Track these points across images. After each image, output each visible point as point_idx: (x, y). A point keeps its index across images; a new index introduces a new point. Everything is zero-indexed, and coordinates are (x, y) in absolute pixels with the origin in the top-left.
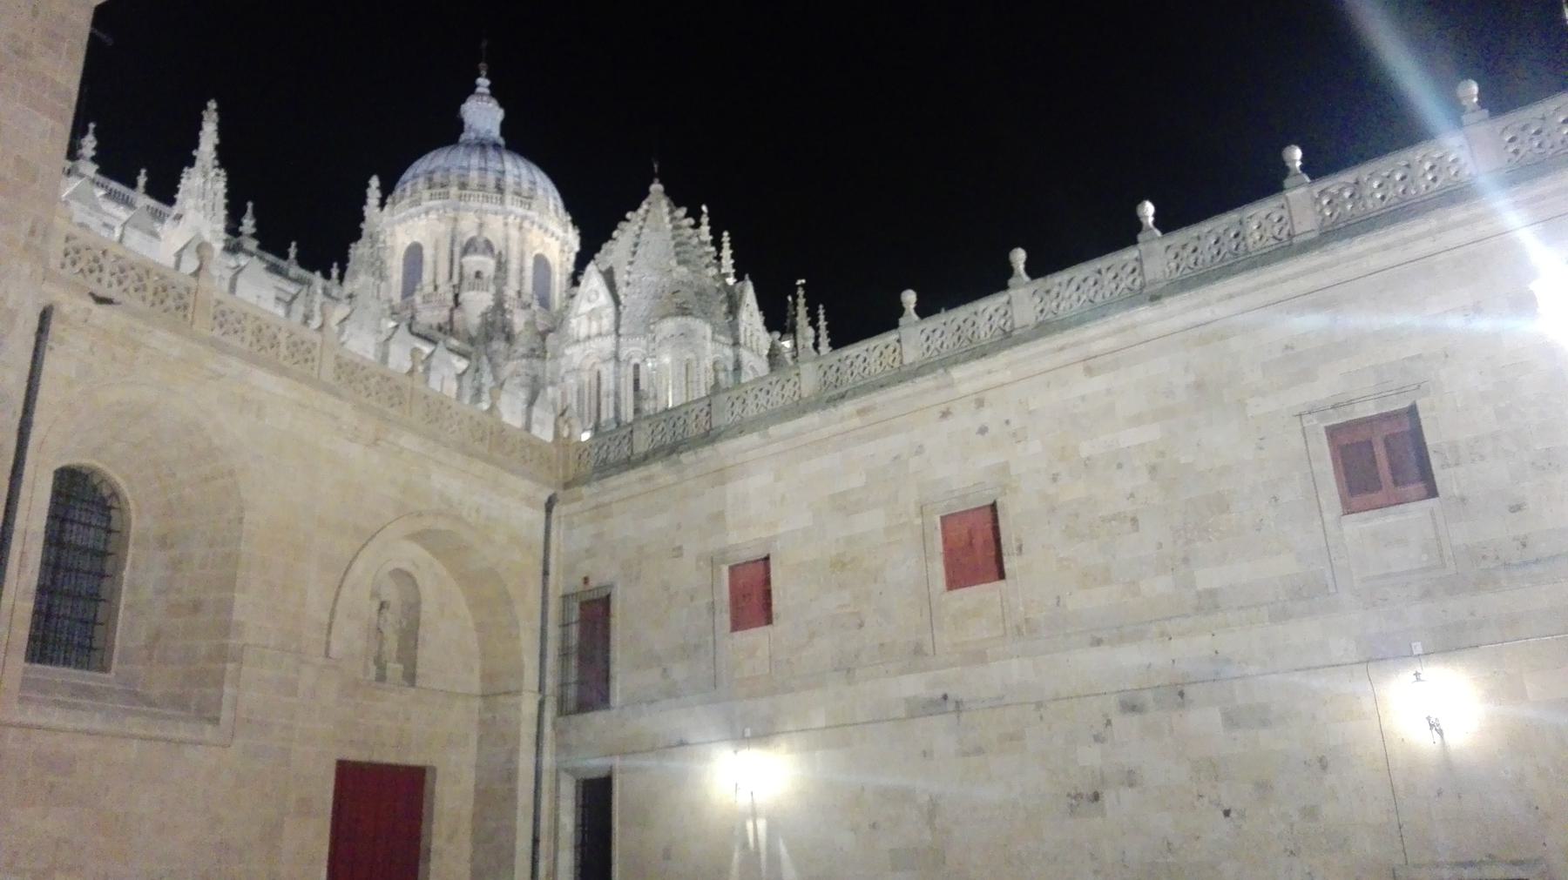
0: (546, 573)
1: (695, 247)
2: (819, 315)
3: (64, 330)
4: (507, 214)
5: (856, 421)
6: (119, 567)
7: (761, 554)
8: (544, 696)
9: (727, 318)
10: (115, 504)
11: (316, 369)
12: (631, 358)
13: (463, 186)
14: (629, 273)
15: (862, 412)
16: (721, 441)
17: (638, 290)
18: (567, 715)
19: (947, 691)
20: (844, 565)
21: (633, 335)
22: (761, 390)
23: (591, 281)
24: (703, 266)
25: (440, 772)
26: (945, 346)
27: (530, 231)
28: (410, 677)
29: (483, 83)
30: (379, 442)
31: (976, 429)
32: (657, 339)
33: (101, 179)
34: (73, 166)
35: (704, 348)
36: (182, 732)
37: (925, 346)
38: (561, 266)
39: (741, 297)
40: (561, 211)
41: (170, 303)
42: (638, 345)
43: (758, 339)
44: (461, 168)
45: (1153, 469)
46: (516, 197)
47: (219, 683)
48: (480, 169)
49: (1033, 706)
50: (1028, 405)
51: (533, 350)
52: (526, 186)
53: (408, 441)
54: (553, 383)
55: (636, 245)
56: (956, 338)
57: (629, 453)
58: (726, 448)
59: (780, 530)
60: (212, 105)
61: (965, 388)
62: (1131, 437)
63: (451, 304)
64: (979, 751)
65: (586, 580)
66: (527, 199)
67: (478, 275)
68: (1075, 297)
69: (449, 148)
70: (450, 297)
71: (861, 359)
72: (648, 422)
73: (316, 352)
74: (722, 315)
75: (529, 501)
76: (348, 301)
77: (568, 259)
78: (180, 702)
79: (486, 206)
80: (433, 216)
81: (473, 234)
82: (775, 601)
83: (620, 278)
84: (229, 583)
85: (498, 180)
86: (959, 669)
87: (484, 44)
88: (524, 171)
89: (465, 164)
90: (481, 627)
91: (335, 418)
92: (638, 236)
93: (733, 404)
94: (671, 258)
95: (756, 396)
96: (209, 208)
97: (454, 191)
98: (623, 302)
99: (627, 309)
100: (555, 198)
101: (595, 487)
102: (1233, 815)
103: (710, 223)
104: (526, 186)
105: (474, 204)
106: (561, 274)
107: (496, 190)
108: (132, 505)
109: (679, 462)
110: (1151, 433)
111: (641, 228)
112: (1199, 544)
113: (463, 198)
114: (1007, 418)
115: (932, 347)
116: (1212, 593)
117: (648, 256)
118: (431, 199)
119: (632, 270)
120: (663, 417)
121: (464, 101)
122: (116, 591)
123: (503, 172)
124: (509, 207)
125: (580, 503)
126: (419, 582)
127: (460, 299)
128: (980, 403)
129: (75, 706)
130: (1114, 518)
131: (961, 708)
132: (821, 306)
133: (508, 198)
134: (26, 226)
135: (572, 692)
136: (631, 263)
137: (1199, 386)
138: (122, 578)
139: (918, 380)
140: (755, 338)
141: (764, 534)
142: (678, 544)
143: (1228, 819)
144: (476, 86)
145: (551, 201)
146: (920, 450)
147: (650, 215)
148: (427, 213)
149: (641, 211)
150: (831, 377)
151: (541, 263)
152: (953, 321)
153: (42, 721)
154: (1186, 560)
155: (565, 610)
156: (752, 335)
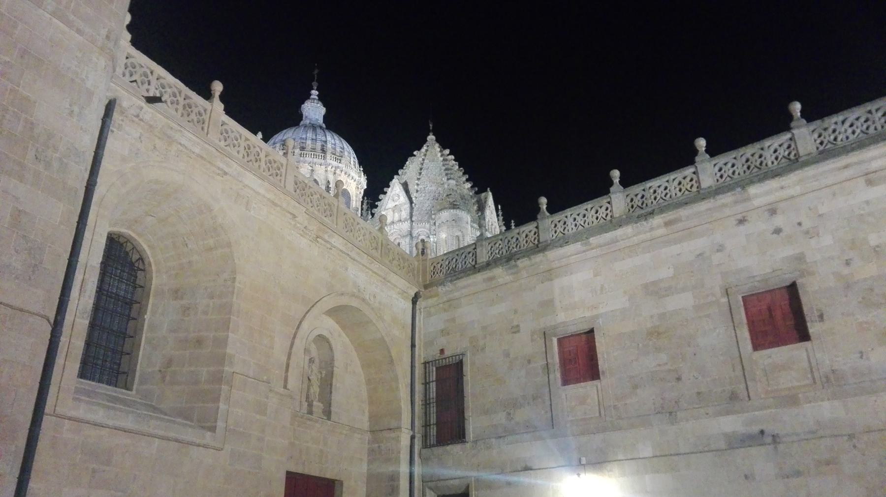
0: (413, 346)
1: (456, 171)
2: (511, 226)
4: (327, 165)
5: (662, 231)
6: (142, 311)
7: (586, 327)
8: (414, 432)
9: (477, 214)
10: (141, 267)
11: (283, 182)
12: (419, 235)
13: (303, 149)
14: (418, 185)
15: (667, 224)
16: (552, 249)
17: (423, 195)
18: (430, 447)
20: (659, 334)
21: (421, 221)
22: (578, 215)
23: (395, 189)
24: (462, 182)
25: (345, 484)
26: (737, 173)
27: (340, 175)
28: (328, 413)
29: (315, 93)
30: (318, 239)
32: (437, 224)
35: (467, 229)
36: (189, 434)
37: (719, 174)
38: (356, 197)
39: (485, 202)
40: (357, 165)
41: (193, 116)
42: (424, 228)
43: (495, 228)
44: (301, 138)
47: (217, 400)
48: (312, 139)
49: (846, 438)
52: (338, 150)
53: (337, 241)
55: (421, 169)
56: (745, 167)
57: (473, 263)
58: (552, 254)
59: (602, 310)
61: (756, 202)
64: (798, 474)
65: (442, 351)
66: (339, 159)
68: (850, 130)
69: (294, 129)
71: (662, 188)
72: (488, 241)
73: (283, 170)
74: (474, 211)
75: (403, 293)
77: (360, 193)
78: (185, 414)
79: (315, 160)
82: (600, 362)
83: (412, 188)
84: (225, 325)
85: (323, 146)
86: (773, 411)
87: (316, 72)
88: (337, 142)
89: (304, 136)
90: (369, 382)
91: (294, 216)
92: (422, 164)
93: (556, 226)
94: (443, 177)
95: (575, 219)
98: (414, 202)
99: (417, 206)
100: (354, 158)
101: (449, 287)
104: (338, 150)
105: (308, 159)
106: (356, 202)
107: (321, 151)
108: (153, 268)
109: (516, 266)
111: (423, 160)
113: (302, 155)
114: (799, 221)
115: (725, 176)
117: (429, 175)
119: (419, 183)
120: (500, 237)
121: (303, 103)
122: (138, 330)
123: (326, 142)
124: (329, 161)
125: (435, 299)
126: (334, 346)
128: (773, 212)
129: (113, 408)
131: (778, 440)
132: (513, 221)
133: (328, 156)
134: (104, 32)
135: (433, 431)
136: (418, 179)
138: (144, 320)
139: (718, 197)
140: (493, 227)
141: (588, 314)
142: (515, 323)
144: (311, 95)
145: (352, 159)
147: (428, 153)
149: (423, 150)
150: (637, 201)
152: (742, 156)
153: (90, 417)
155: (426, 374)
156: (492, 225)
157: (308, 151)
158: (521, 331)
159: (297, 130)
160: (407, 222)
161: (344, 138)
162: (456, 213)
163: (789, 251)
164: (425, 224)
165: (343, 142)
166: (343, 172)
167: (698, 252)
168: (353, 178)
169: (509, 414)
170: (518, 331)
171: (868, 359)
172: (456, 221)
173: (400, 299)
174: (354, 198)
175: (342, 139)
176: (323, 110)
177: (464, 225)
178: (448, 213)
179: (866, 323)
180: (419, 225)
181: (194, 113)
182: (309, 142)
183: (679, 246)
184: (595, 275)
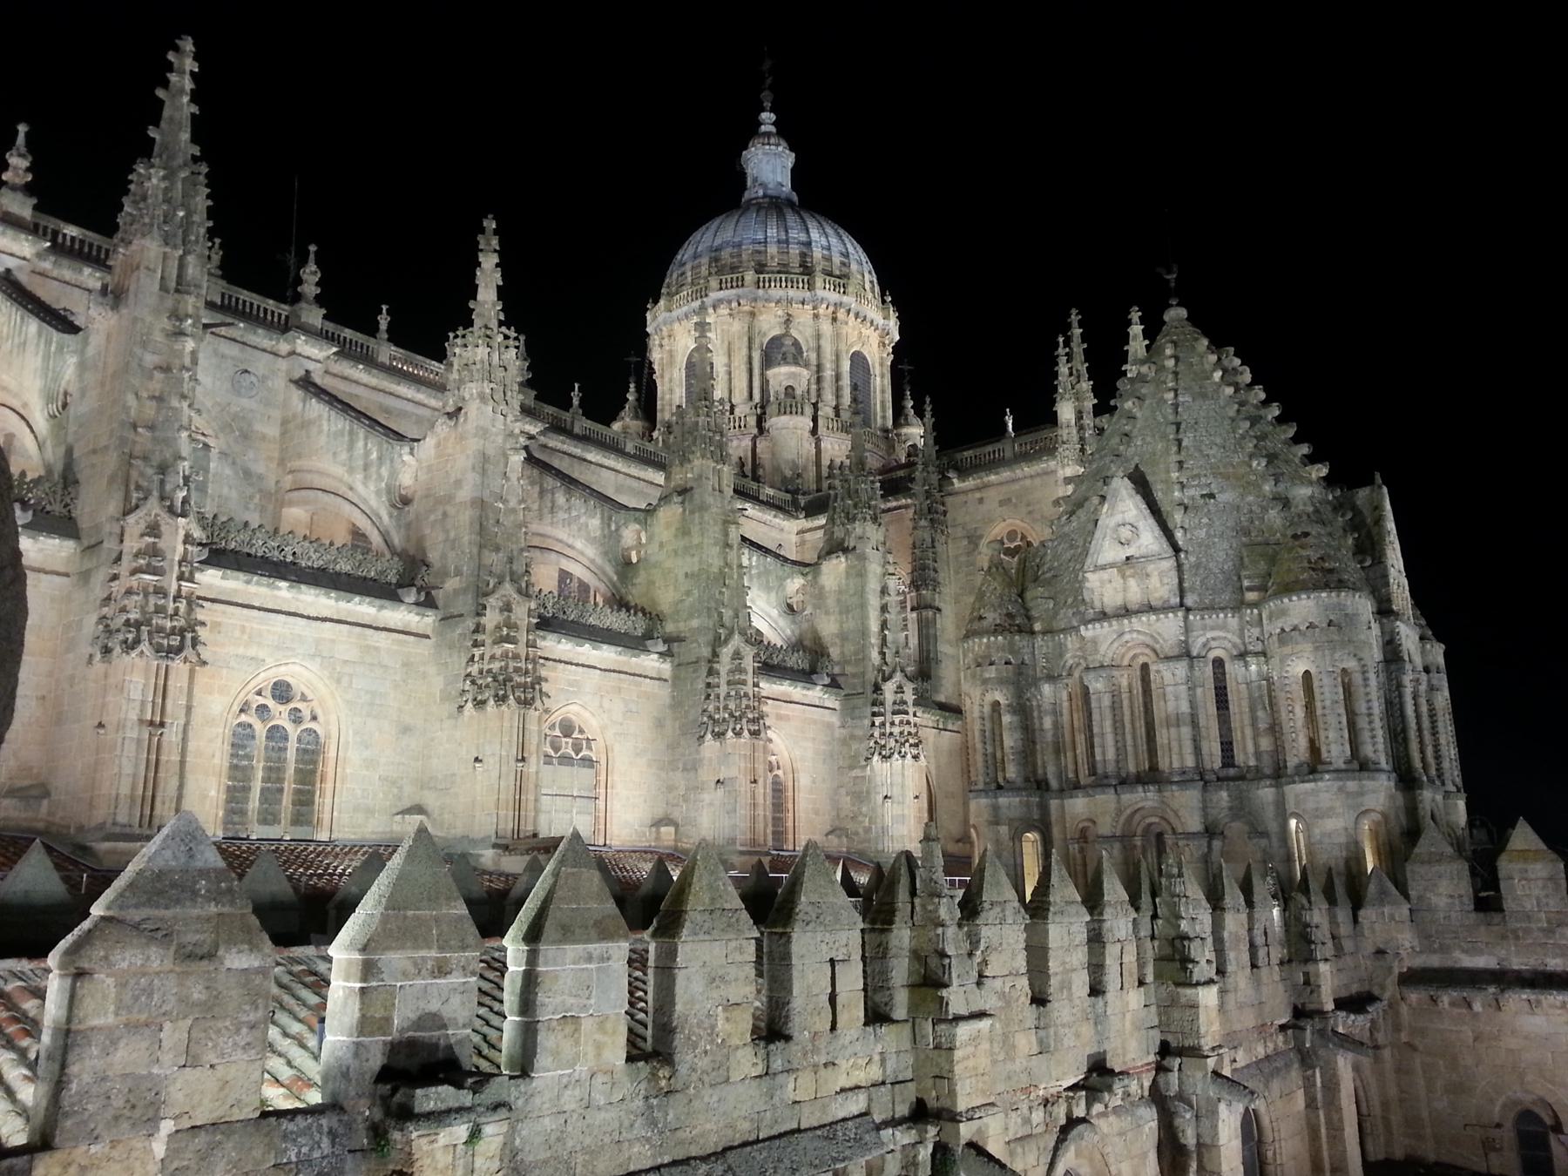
13: (760, 268)
21: (1212, 608)
23: (1121, 506)
27: (847, 323)
29: (767, 117)
33: (330, 327)
34: (291, 312)
42: (1224, 627)
44: (755, 242)
46: (828, 278)
48: (779, 242)
51: (1010, 615)
52: (837, 259)
54: (1051, 678)
60: (490, 224)
63: (755, 431)
66: (840, 279)
67: (790, 390)
70: (752, 421)
76: (680, 499)
79: (792, 293)
80: (723, 310)
81: (777, 332)
85: (803, 255)
87: (767, 65)
88: (834, 240)
89: (760, 236)
96: (499, 396)
97: (750, 276)
103: (1142, 320)
104: (837, 259)
105: (776, 292)
106: (882, 376)
118: (721, 289)
121: (746, 148)
123: (809, 244)
124: (820, 293)
127: (767, 425)
133: (819, 282)
145: (867, 276)
148: (715, 308)
151: (858, 360)
157: (773, 272)
159: (742, 220)
160: (1176, 616)
161: (846, 229)
162: (1335, 600)
164: (1226, 616)
165: (844, 238)
166: (852, 315)
168: (872, 323)
172: (1340, 628)
174: (878, 371)
175: (841, 231)
176: (789, 159)
177: (1362, 637)
178: (1311, 603)
180: (1208, 621)
182: (772, 249)
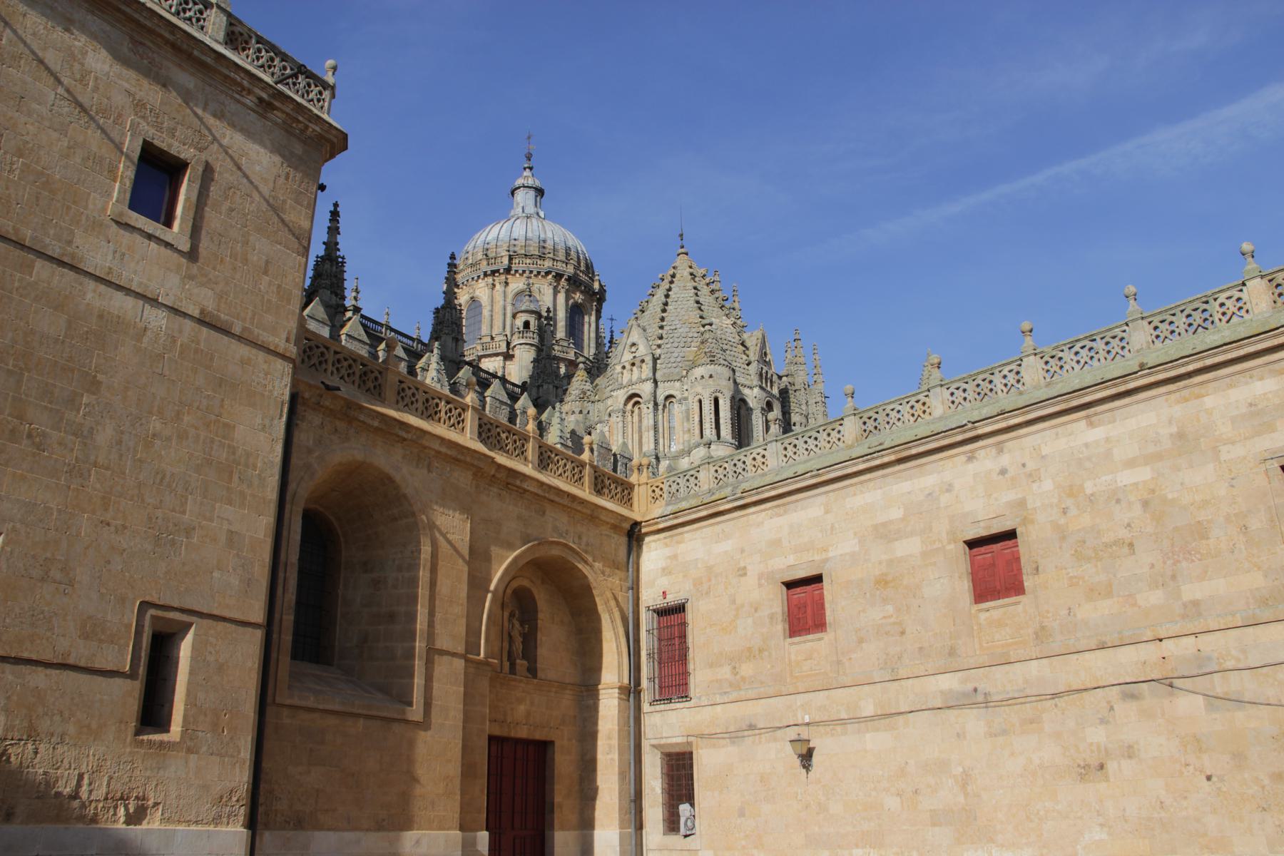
3: (305, 411)
19: (977, 685)
20: (886, 583)
25: (557, 744)
31: (998, 470)
41: (370, 384)
45: (1145, 504)
50: (1040, 450)
59: (831, 554)
62: (1126, 478)
64: (1004, 732)
102: (1214, 779)
110: (1143, 474)
112: (1184, 564)
116: (1196, 603)
130: (1116, 543)
134: (284, 336)
137: (1181, 436)
142: (742, 565)
143: (1210, 783)
146: (949, 488)
153: (303, 703)
154: (1174, 577)
158: (748, 574)
163: (1012, 496)
167: (927, 492)
169: (735, 668)
170: (745, 574)
171: (1075, 615)
173: (613, 535)
179: (1075, 577)
181: (370, 380)
183: (909, 482)
184: (827, 512)
